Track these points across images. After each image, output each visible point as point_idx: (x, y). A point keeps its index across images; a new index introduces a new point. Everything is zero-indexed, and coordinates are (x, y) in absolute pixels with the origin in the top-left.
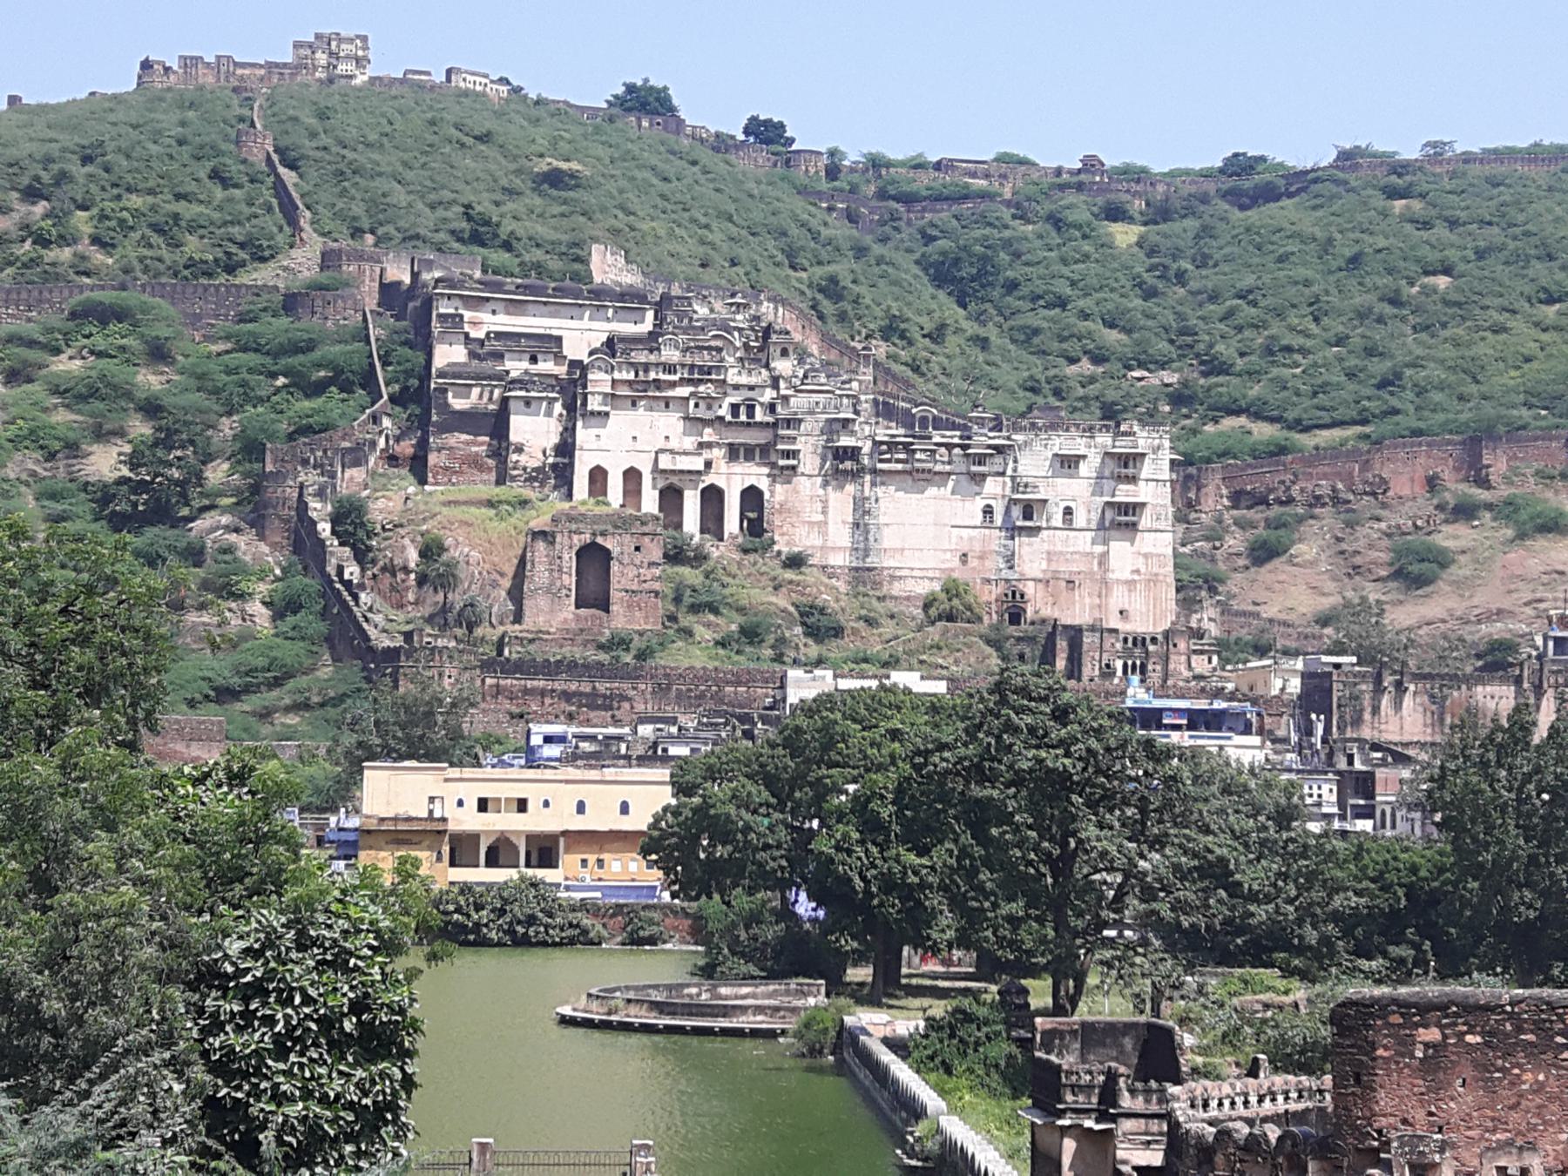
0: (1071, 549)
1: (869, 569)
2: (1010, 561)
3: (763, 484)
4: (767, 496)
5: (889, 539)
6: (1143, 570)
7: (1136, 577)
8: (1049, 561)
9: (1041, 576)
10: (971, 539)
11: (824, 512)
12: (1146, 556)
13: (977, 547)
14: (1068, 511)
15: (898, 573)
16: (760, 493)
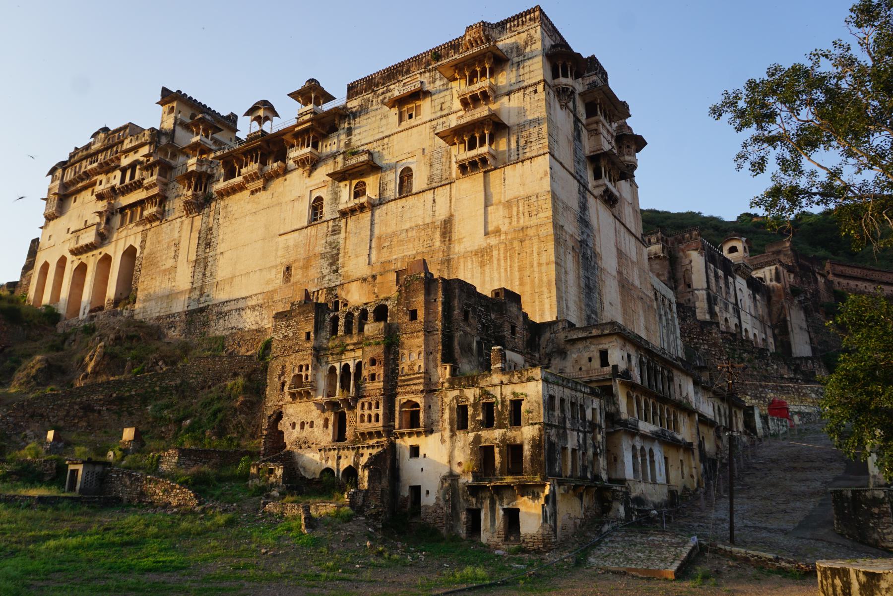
0: (407, 226)
1: (202, 310)
2: (334, 260)
3: (137, 246)
4: (138, 255)
5: (223, 269)
6: (504, 229)
7: (493, 241)
8: (380, 248)
9: (366, 271)
10: (296, 246)
11: (176, 257)
12: (508, 204)
13: (302, 254)
14: (406, 175)
15: (226, 309)
16: (136, 250)
